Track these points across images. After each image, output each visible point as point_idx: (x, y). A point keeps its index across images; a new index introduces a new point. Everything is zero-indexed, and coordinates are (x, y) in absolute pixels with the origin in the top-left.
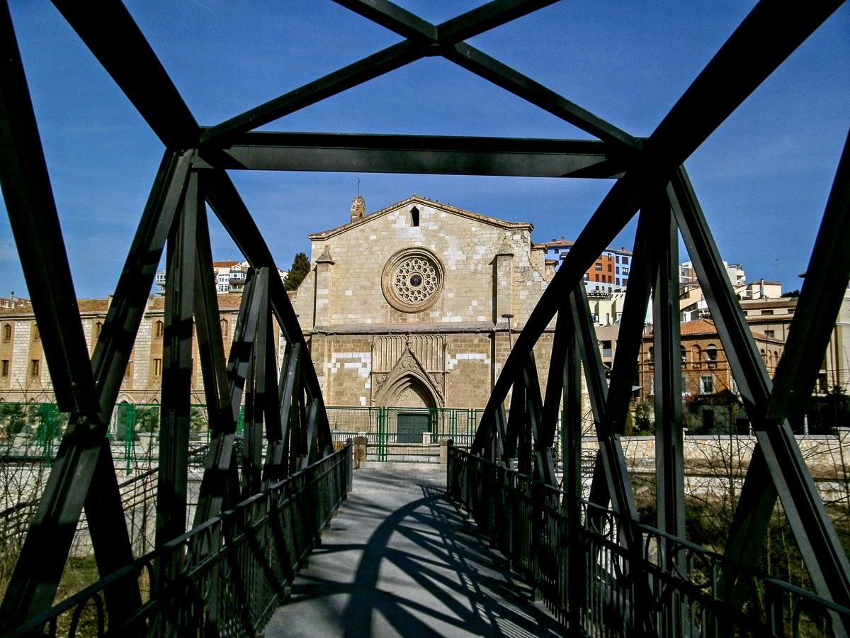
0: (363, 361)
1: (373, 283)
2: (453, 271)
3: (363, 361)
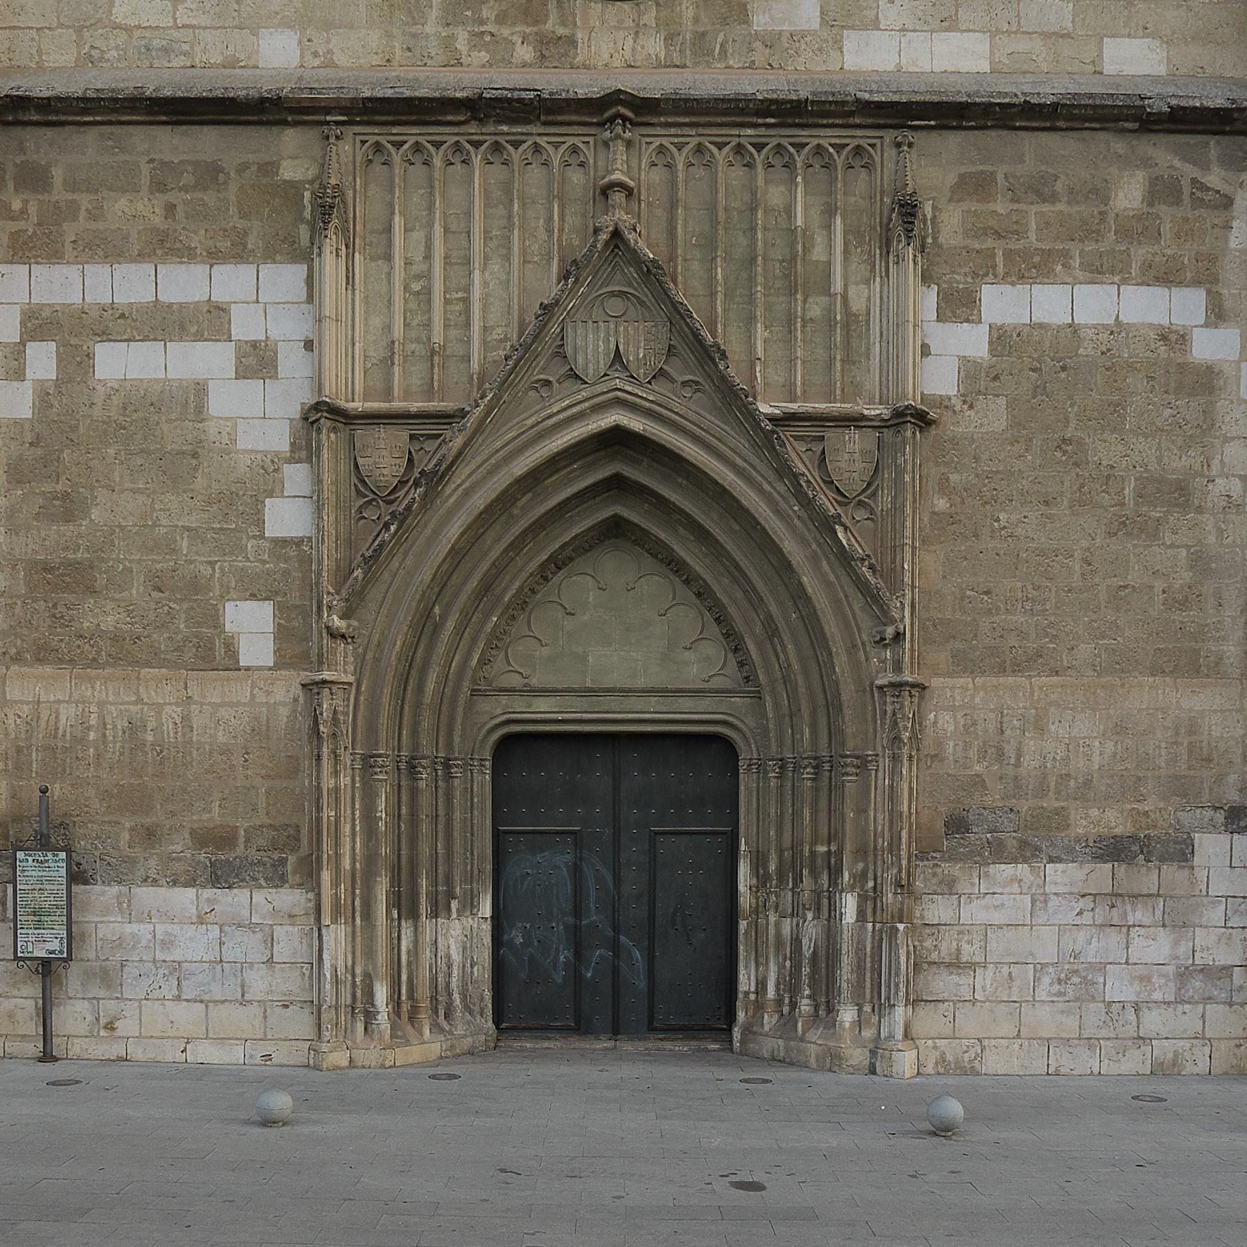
0: (245, 326)
3: (245, 326)
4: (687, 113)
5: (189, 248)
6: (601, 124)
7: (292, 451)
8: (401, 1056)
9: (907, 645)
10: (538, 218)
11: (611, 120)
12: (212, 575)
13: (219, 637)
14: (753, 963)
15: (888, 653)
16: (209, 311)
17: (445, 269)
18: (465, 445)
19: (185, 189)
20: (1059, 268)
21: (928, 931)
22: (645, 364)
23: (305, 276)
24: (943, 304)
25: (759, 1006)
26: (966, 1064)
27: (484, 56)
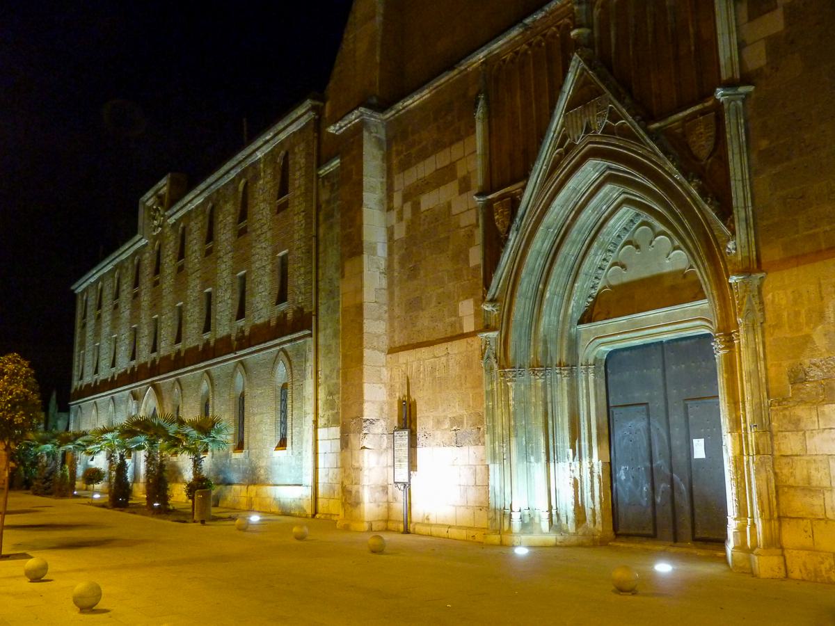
21: (784, 460)
26: (824, 573)
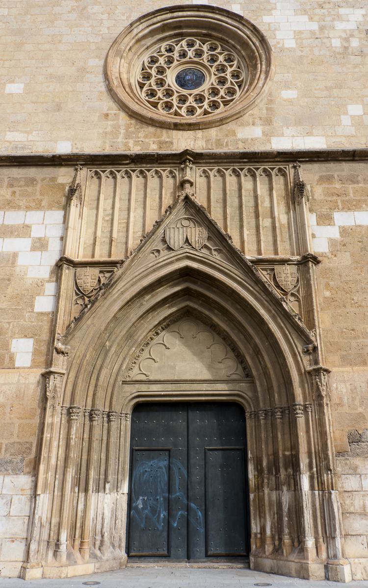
1: (83, 70)
2: (288, 49)
3: (37, 232)
4: (213, 159)
5: (19, 206)
6: (181, 163)
7: (50, 278)
8: (71, 571)
9: (320, 352)
10: (156, 195)
11: (185, 162)
12: (9, 328)
13: (8, 354)
14: (258, 517)
15: (311, 357)
16: (23, 227)
17: (119, 212)
18: (122, 274)
19: (21, 186)
20: (364, 206)
22: (198, 243)
23: (63, 214)
24: (319, 220)
25: (263, 541)
27: (139, 148)
